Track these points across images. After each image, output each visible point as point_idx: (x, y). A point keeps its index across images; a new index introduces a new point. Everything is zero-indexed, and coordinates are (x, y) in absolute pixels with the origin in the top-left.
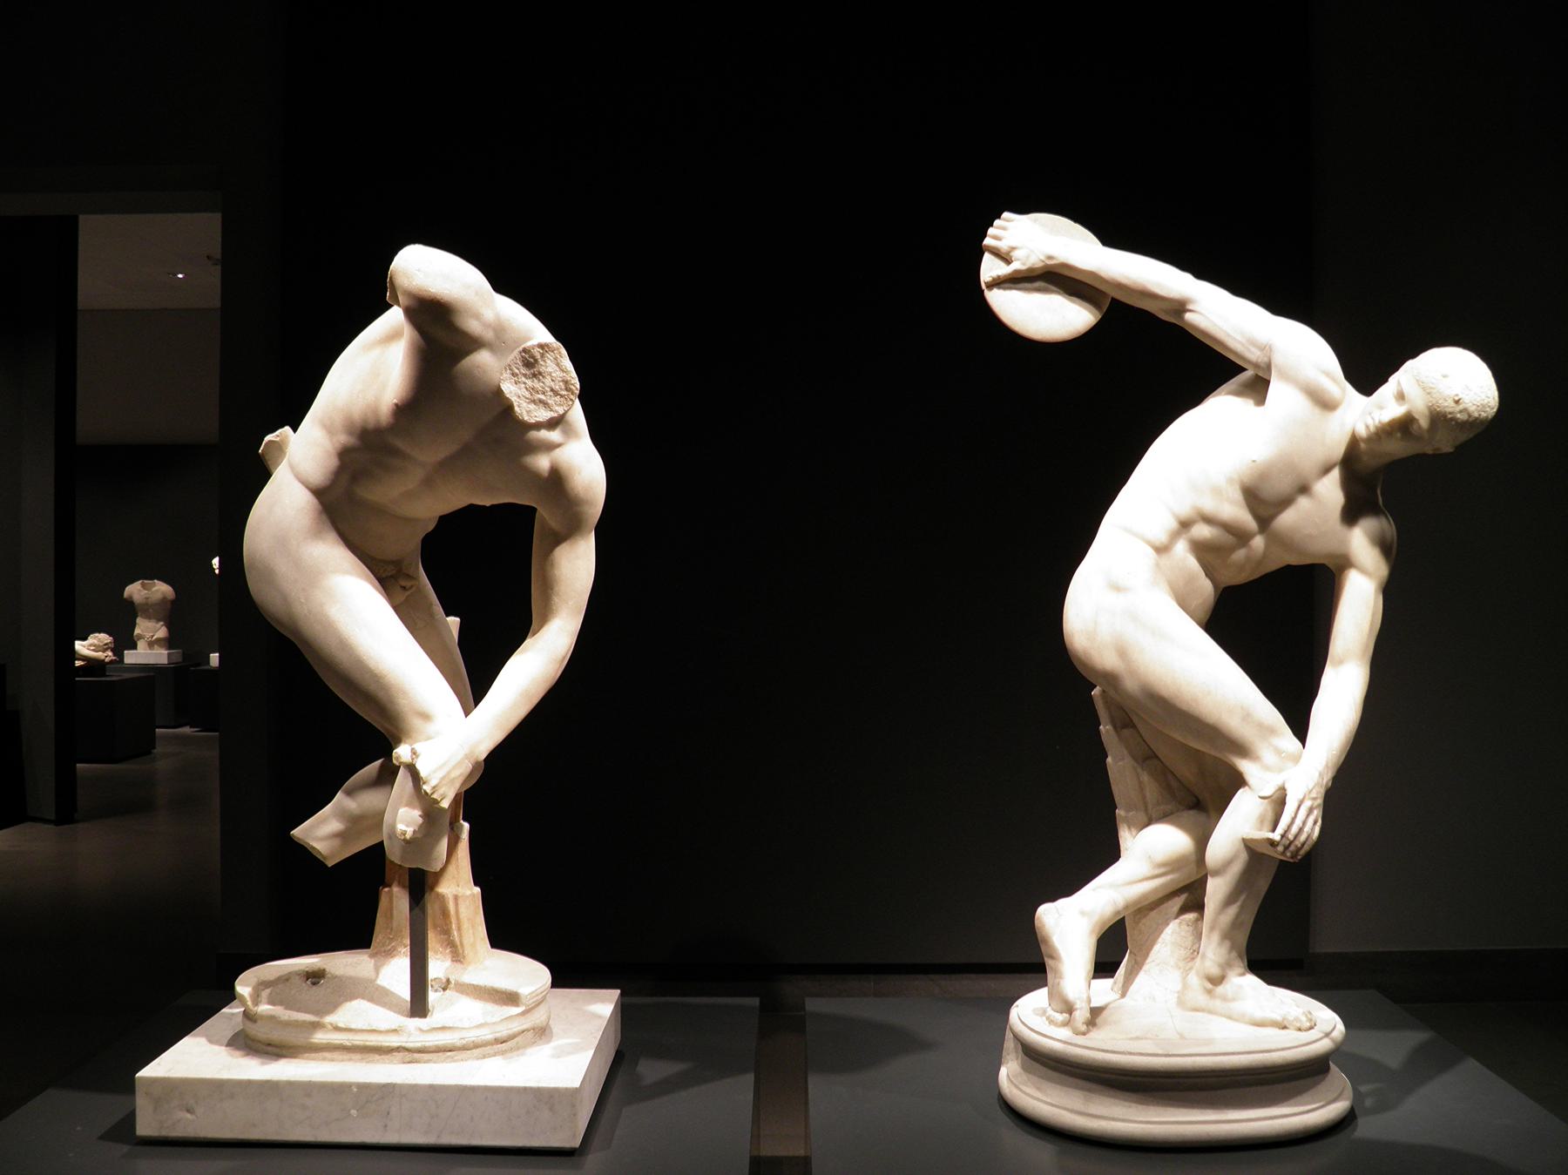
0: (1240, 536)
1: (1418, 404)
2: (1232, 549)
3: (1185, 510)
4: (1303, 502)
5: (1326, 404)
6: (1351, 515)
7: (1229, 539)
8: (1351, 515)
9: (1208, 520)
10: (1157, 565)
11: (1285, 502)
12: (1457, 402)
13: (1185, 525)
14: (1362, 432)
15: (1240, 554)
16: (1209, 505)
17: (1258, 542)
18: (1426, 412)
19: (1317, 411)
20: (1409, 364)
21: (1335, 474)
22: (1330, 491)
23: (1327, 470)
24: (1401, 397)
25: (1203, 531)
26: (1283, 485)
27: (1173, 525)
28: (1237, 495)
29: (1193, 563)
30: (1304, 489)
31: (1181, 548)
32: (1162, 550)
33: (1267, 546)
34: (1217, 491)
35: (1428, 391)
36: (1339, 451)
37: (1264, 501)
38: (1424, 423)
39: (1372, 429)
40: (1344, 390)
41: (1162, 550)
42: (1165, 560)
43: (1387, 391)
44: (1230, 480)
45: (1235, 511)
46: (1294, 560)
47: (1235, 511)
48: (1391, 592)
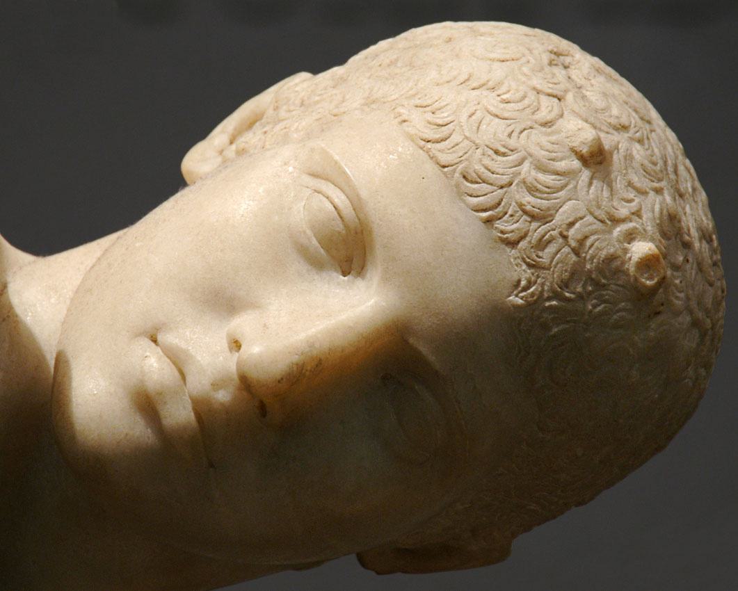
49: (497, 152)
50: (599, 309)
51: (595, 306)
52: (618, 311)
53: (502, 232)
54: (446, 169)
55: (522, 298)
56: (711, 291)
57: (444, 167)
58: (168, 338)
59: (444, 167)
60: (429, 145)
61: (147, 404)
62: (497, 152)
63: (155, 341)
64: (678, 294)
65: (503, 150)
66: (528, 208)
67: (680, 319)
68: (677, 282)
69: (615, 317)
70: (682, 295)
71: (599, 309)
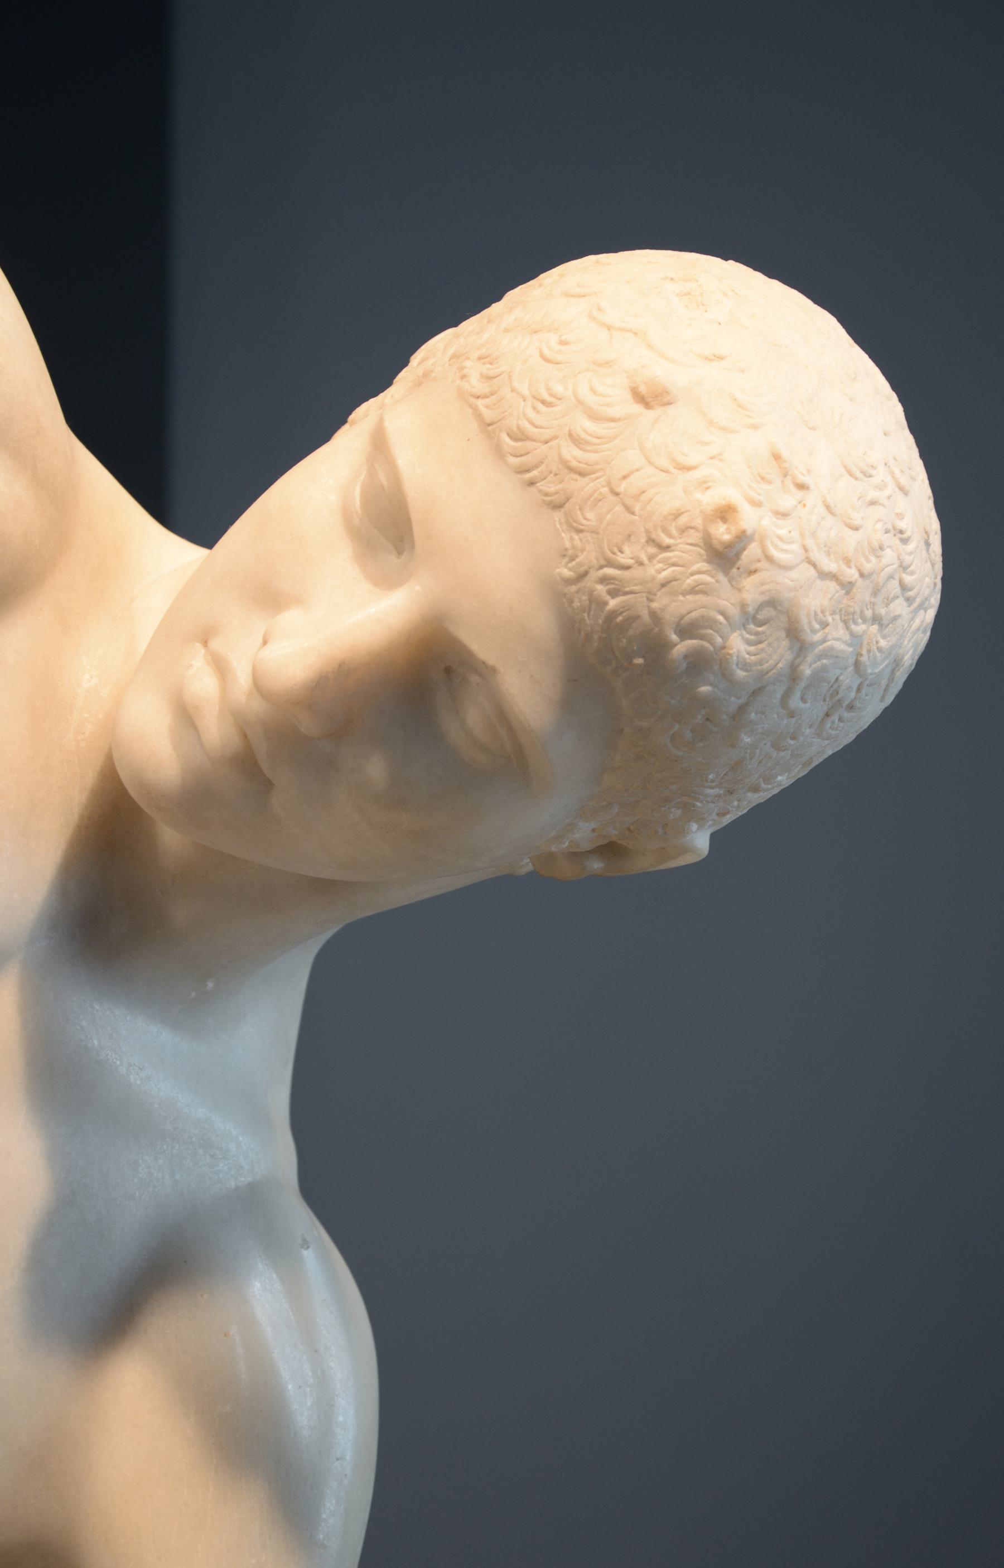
1: (494, 574)
12: (725, 557)
14: (156, 752)
20: (438, 350)
24: (388, 529)
40: (57, 497)
49: (544, 402)
50: (664, 574)
51: (659, 572)
52: (692, 574)
53: (546, 495)
54: (490, 428)
55: (570, 569)
56: (852, 539)
57: (489, 425)
59: (489, 425)
60: (480, 403)
62: (544, 402)
64: (786, 547)
65: (549, 399)
66: (574, 464)
67: (794, 574)
68: (783, 532)
69: (689, 581)
70: (794, 547)
71: (664, 574)
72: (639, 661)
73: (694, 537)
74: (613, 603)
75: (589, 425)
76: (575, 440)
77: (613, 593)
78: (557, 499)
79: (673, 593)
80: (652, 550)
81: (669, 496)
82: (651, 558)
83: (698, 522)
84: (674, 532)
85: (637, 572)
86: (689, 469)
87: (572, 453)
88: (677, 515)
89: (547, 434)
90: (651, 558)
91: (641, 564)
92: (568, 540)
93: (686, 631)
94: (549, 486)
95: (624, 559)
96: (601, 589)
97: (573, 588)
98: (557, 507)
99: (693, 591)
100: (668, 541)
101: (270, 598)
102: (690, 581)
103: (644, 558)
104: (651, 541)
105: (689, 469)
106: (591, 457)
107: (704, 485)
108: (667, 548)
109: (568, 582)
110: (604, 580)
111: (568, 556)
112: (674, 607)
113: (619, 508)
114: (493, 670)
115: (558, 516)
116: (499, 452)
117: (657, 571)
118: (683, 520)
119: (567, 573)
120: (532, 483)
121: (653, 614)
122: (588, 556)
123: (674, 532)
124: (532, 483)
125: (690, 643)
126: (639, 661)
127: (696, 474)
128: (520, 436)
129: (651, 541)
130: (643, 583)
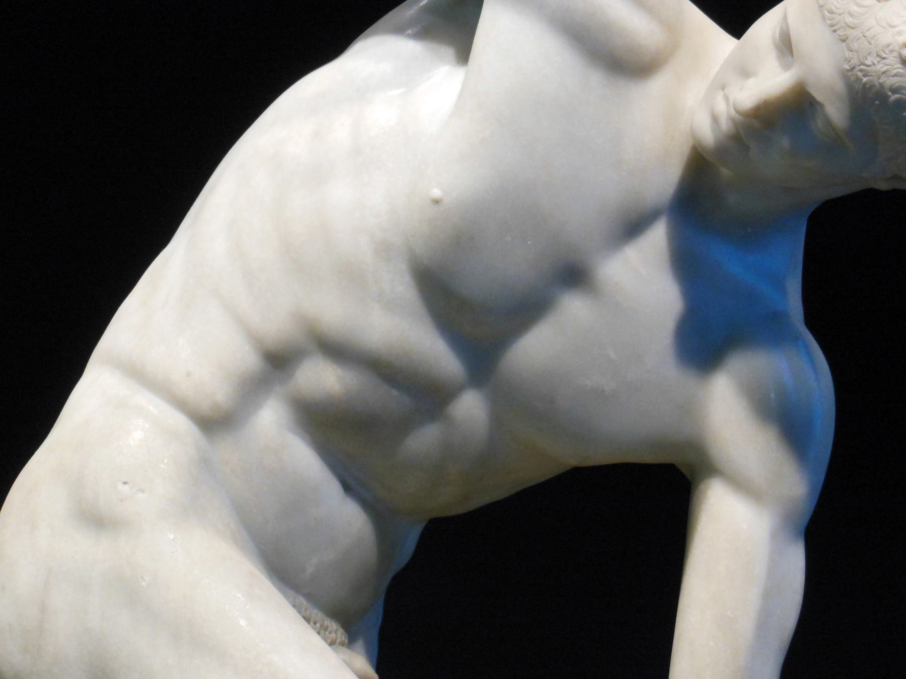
0: (427, 396)
1: (822, 66)
2: (405, 425)
3: (276, 324)
4: (573, 308)
5: (622, 62)
6: (704, 341)
7: (389, 400)
8: (704, 341)
9: (335, 350)
10: (205, 463)
11: (528, 309)
13: (278, 361)
14: (708, 135)
15: (424, 439)
16: (334, 311)
17: (470, 408)
18: (840, 86)
19: (596, 78)
21: (657, 237)
22: (643, 279)
23: (632, 227)
24: (786, 46)
25: (322, 378)
26: (511, 263)
27: (247, 359)
28: (403, 287)
29: (303, 459)
30: (574, 275)
31: (271, 420)
32: (215, 423)
33: (497, 420)
34: (351, 276)
35: (841, 32)
36: (664, 179)
37: (481, 295)
38: (836, 112)
39: (725, 125)
40: (673, 28)
41: (215, 423)
42: (227, 452)
43: (765, 26)
44: (384, 250)
45: (401, 328)
46: (569, 455)
47: (401, 328)
48: (831, 534)
58: (726, 90)
61: (715, 119)
63: (723, 89)
72: (877, 102)
73: (895, 54)
74: (865, 80)
75: (856, 9)
76: (851, 15)
77: (865, 76)
78: (844, 38)
79: (888, 76)
80: (878, 59)
81: (886, 38)
82: (879, 62)
83: (897, 48)
84: (887, 52)
85: (873, 68)
86: (894, 27)
87: (849, 20)
88: (888, 46)
89: (840, 11)
90: (879, 62)
91: (874, 64)
92: (848, 54)
93: (895, 90)
94: (840, 33)
95: (868, 62)
96: (860, 74)
97: (850, 74)
98: (844, 41)
99: (895, 75)
100: (884, 56)
101: (745, 73)
102: (895, 72)
103: (876, 62)
104: (878, 56)
105: (894, 27)
106: (856, 21)
107: (900, 33)
108: (885, 58)
109: (848, 71)
110: (861, 70)
111: (848, 60)
112: (889, 81)
113: (866, 42)
114: (820, 105)
115: (844, 44)
116: (824, 18)
117: (880, 67)
118: (891, 48)
119: (848, 67)
120: (835, 31)
121: (881, 85)
122: (855, 61)
123: (887, 52)
124: (835, 31)
125: (897, 96)
126: (877, 102)
127: (896, 29)
128: (831, 12)
129: (878, 56)
130: (876, 72)
